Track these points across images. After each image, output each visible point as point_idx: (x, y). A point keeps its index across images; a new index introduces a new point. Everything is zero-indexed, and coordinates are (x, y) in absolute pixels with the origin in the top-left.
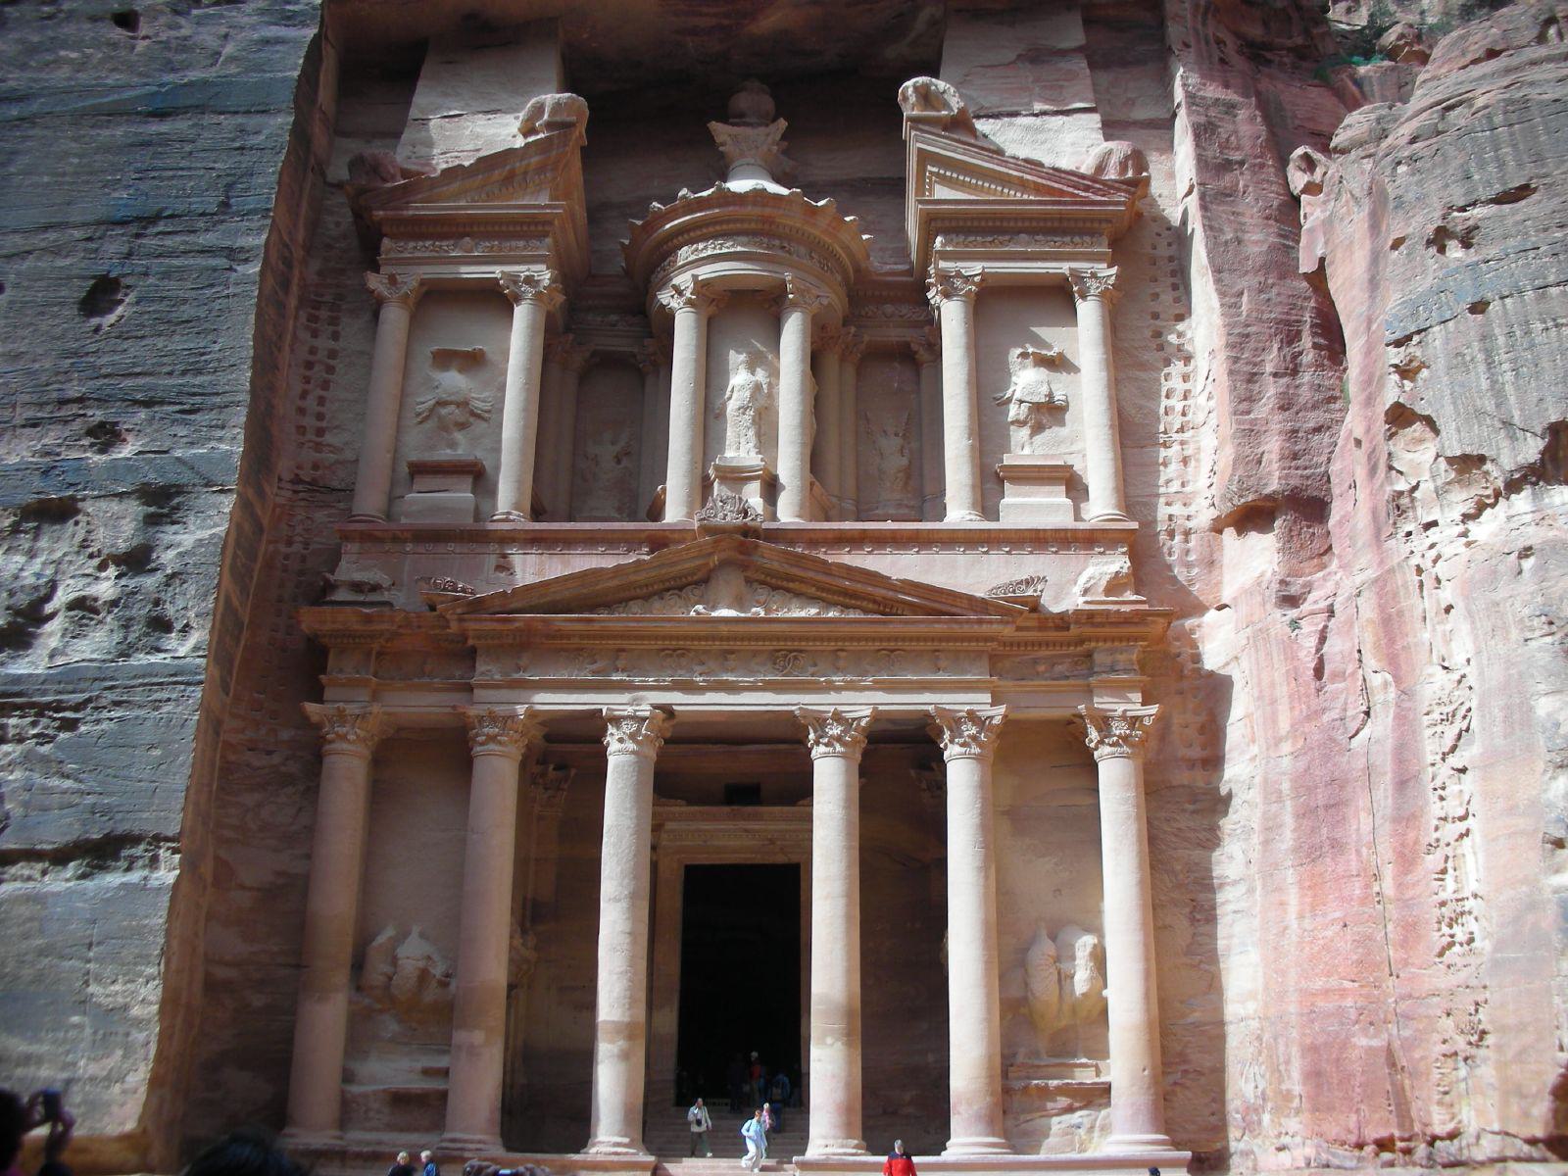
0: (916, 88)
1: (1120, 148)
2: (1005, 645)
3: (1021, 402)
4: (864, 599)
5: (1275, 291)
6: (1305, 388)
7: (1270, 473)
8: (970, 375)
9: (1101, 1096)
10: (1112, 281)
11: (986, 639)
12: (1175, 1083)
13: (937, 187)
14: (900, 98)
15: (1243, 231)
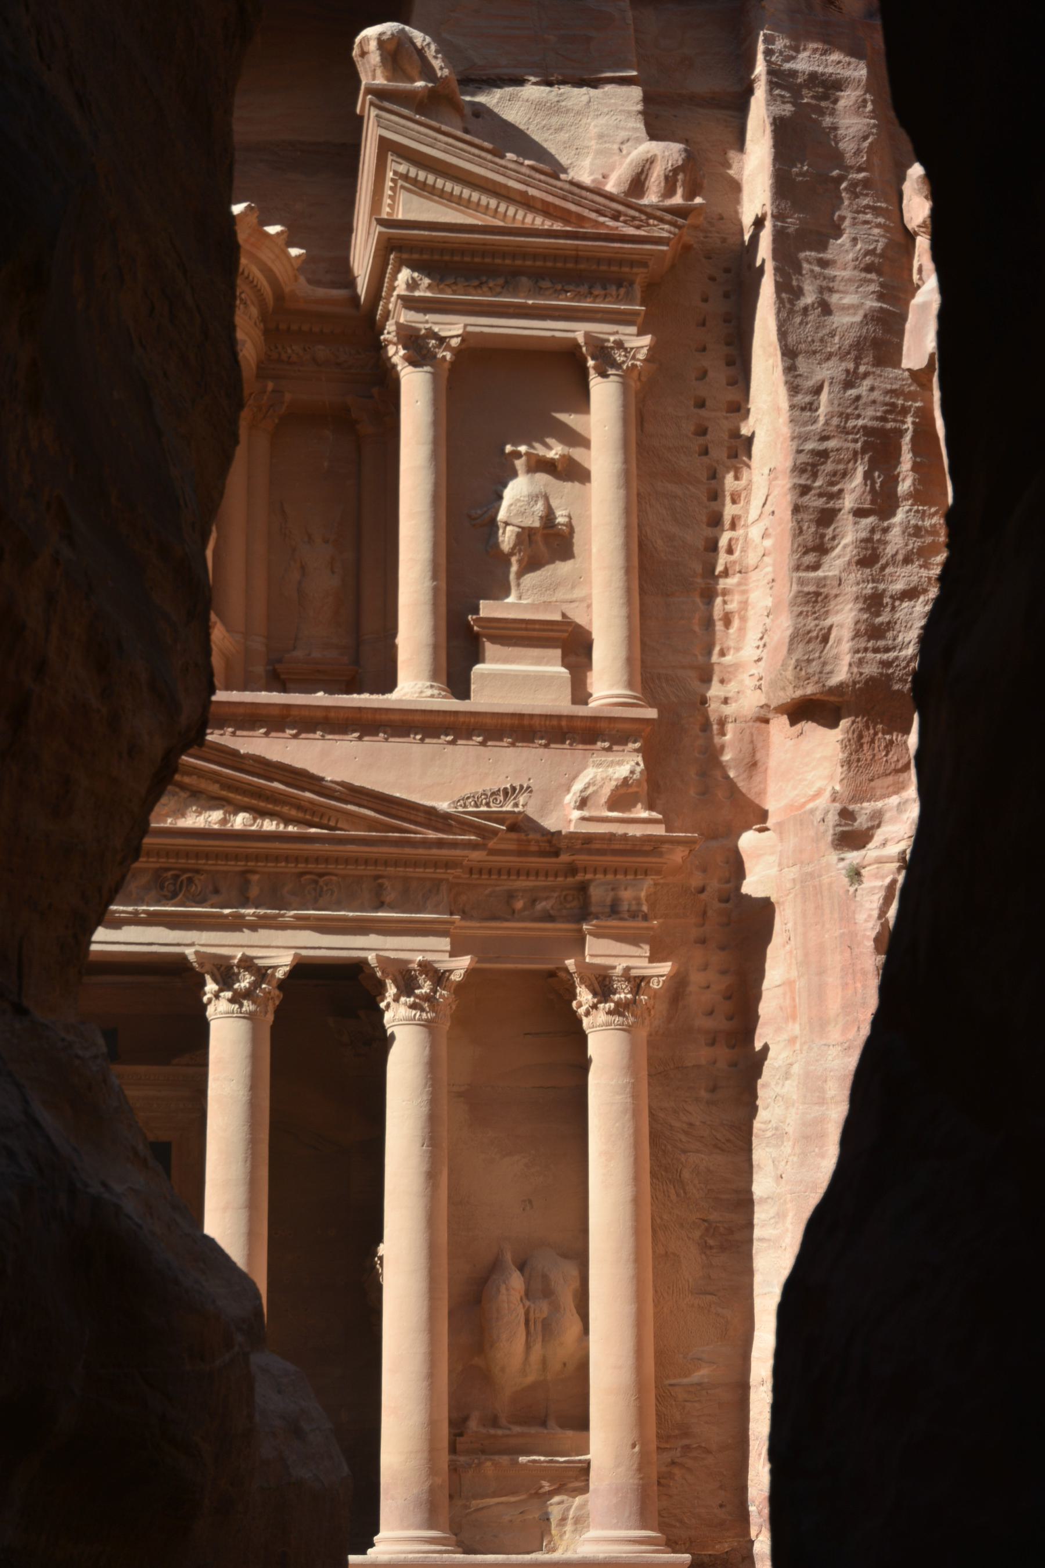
0: (381, 43)
1: (668, 153)
2: (471, 871)
3: (507, 524)
4: (284, 803)
5: (867, 383)
6: (896, 531)
7: (836, 657)
8: (436, 485)
9: (576, 1479)
10: (642, 355)
11: (448, 865)
12: (673, 1463)
13: (403, 196)
14: (356, 52)
15: (831, 290)
